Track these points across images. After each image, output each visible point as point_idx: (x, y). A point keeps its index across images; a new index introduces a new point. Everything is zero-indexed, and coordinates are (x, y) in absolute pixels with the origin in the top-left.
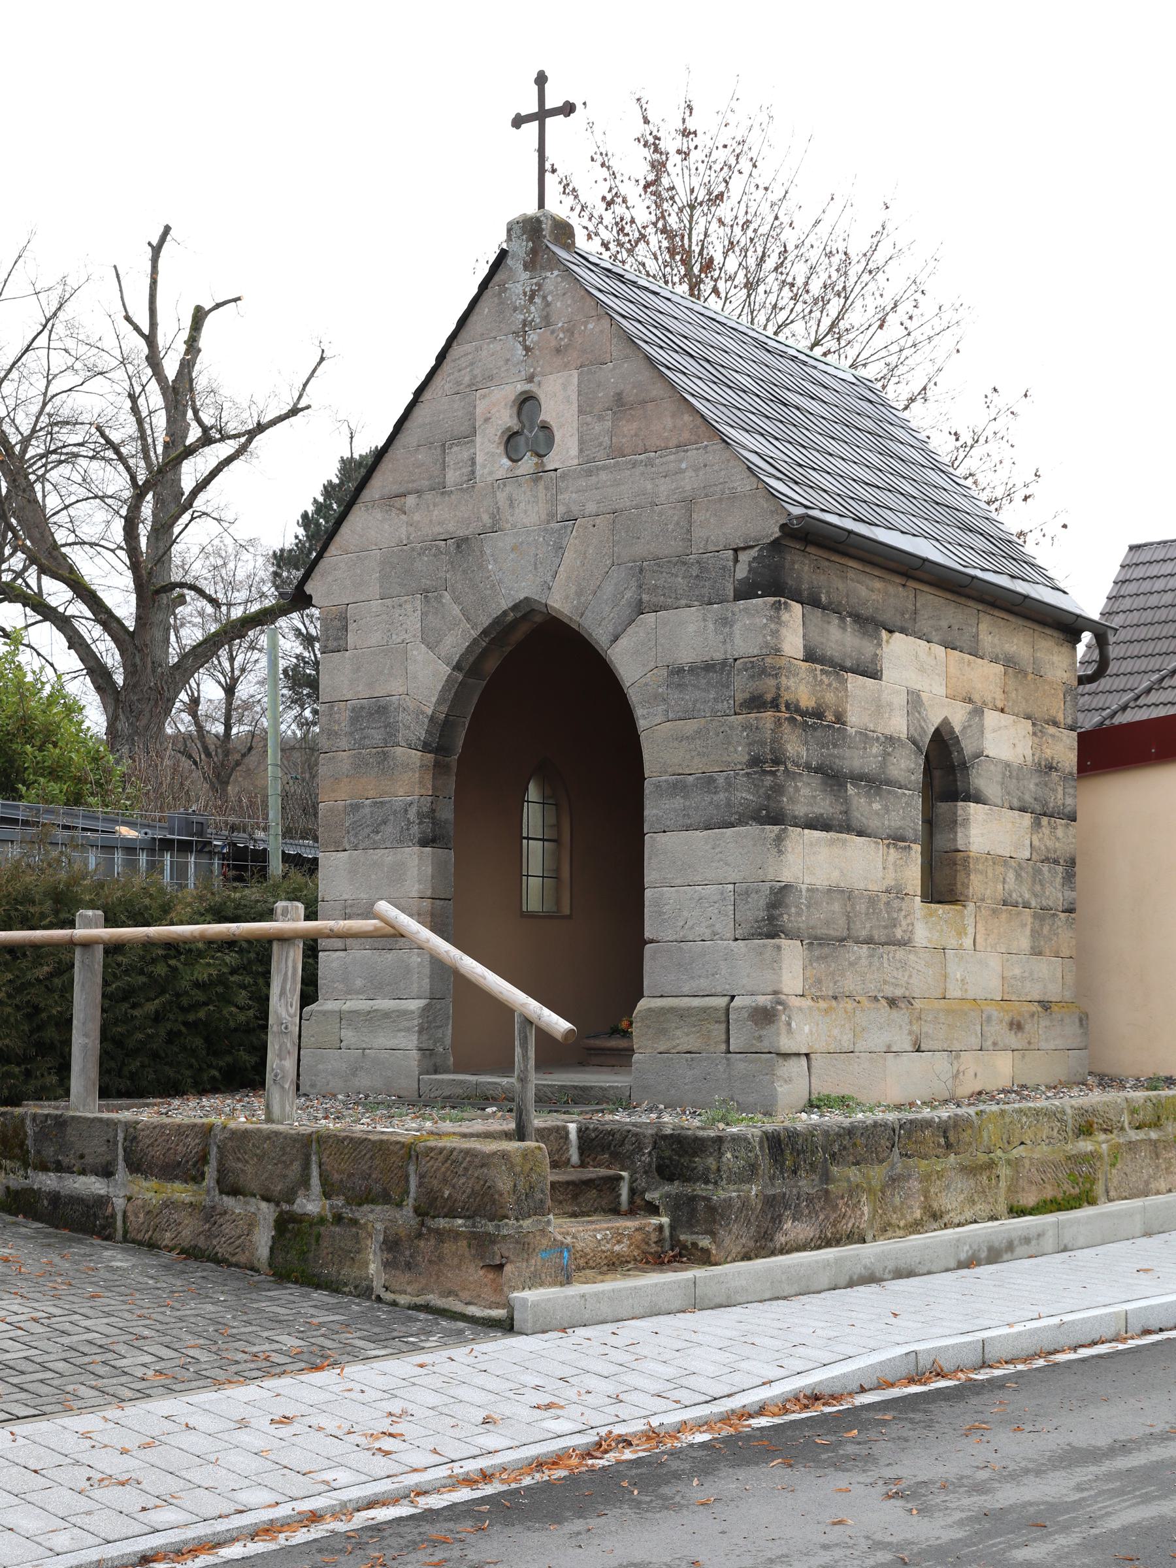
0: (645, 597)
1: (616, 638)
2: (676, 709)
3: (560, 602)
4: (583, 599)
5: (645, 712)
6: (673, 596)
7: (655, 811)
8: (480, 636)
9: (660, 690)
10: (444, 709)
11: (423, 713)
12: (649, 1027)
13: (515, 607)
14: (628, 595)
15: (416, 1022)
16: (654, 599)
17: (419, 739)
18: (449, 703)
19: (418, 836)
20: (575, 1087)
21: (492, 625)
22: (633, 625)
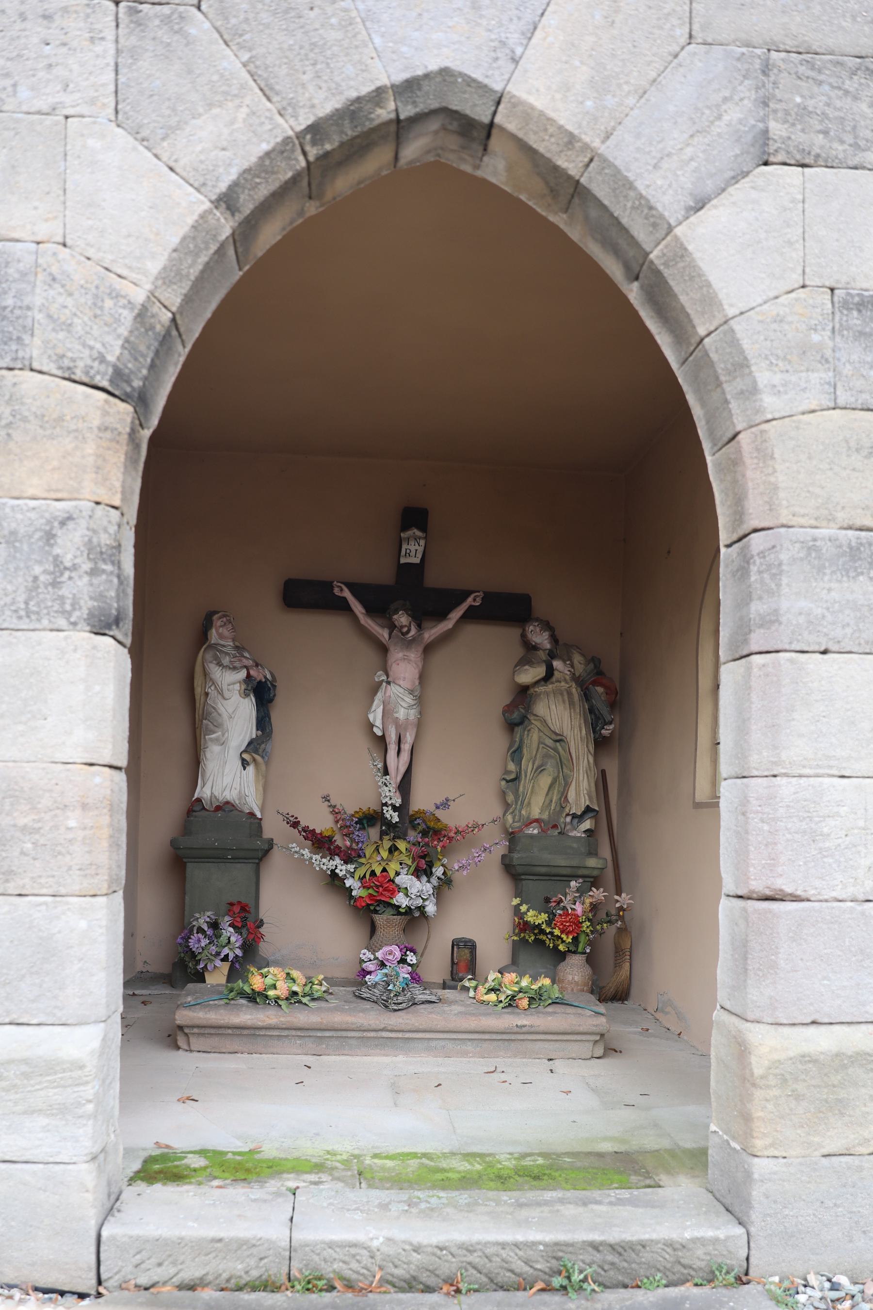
0: (776, 128)
1: (699, 205)
2: (859, 384)
3: (549, 89)
4: (610, 101)
5: (777, 379)
6: (849, 139)
7: (803, 604)
8: (300, 135)
9: (816, 338)
10: (174, 298)
11: (116, 295)
12: (798, 1097)
13: (409, 87)
14: (733, 114)
15: (89, 1091)
16: (800, 138)
17: (102, 359)
18: (186, 286)
19: (87, 604)
20: (595, 1246)
21: (338, 117)
22: (744, 183)
